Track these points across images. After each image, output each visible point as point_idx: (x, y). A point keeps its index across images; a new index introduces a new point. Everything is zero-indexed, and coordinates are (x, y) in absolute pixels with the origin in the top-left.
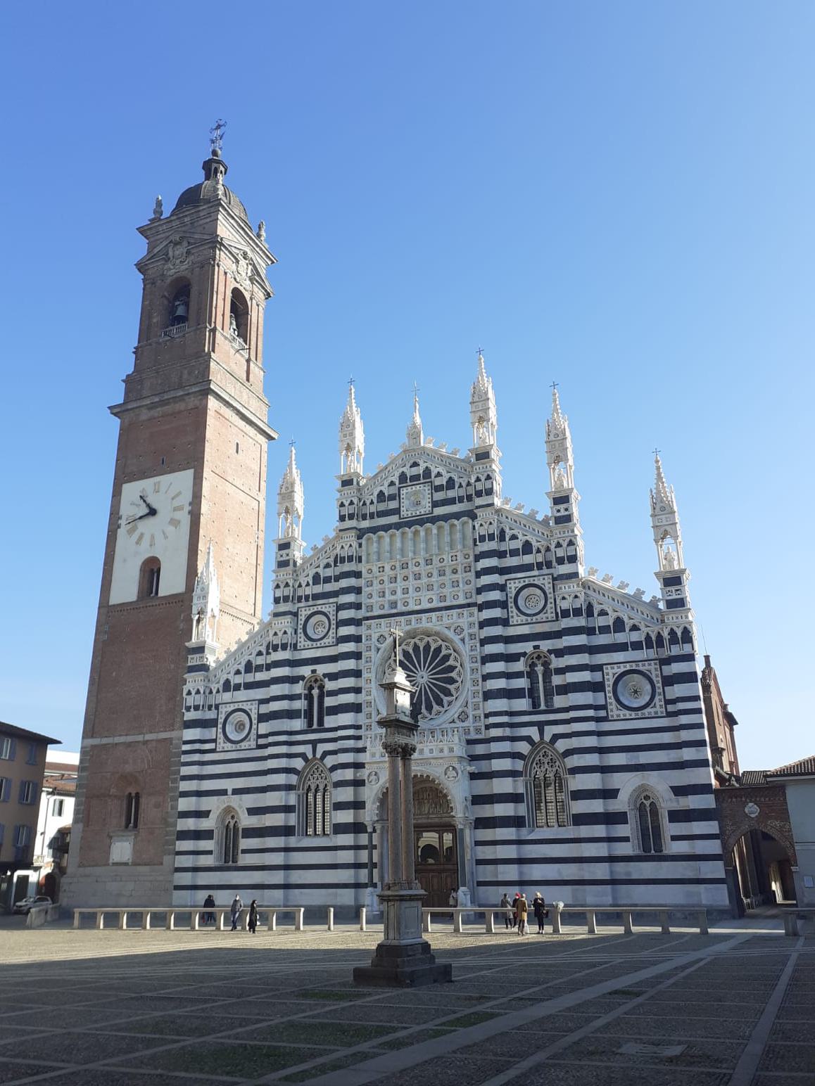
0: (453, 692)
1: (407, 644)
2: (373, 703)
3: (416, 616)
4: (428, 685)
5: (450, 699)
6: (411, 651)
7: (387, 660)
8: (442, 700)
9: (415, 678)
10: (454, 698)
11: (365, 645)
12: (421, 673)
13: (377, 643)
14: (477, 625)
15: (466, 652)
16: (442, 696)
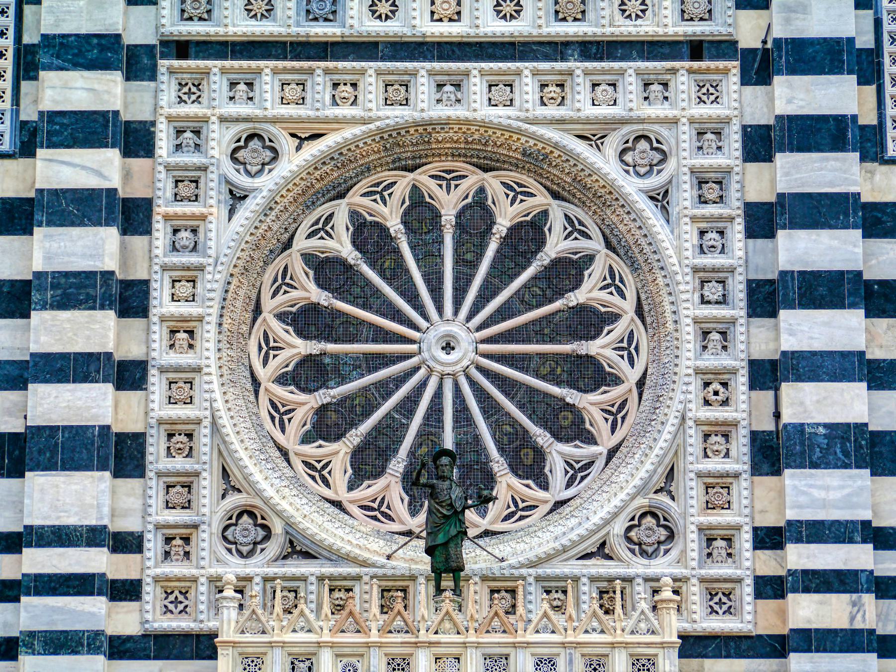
0: (598, 423)
1: (381, 192)
2: (205, 431)
3: (437, 65)
4: (472, 383)
5: (585, 451)
6: (395, 225)
7: (274, 254)
8: (540, 455)
9: (414, 347)
10: (601, 449)
11: (168, 168)
12: (443, 328)
13: (228, 168)
14: (734, 141)
15: (679, 250)
16: (541, 437)
